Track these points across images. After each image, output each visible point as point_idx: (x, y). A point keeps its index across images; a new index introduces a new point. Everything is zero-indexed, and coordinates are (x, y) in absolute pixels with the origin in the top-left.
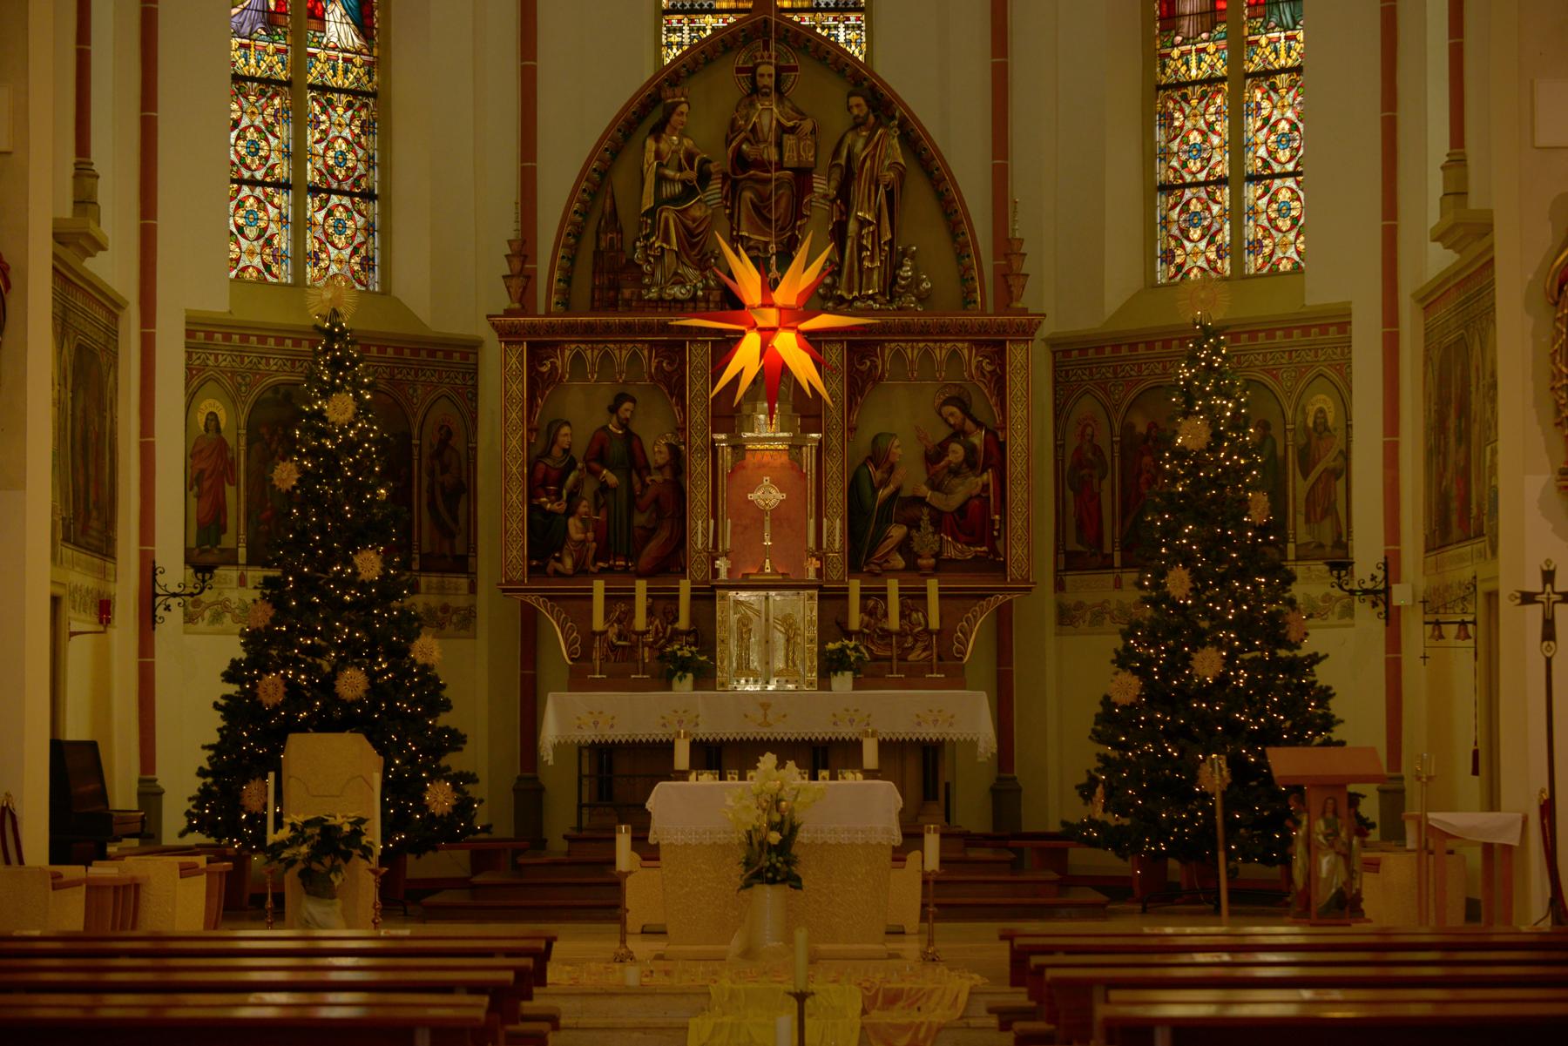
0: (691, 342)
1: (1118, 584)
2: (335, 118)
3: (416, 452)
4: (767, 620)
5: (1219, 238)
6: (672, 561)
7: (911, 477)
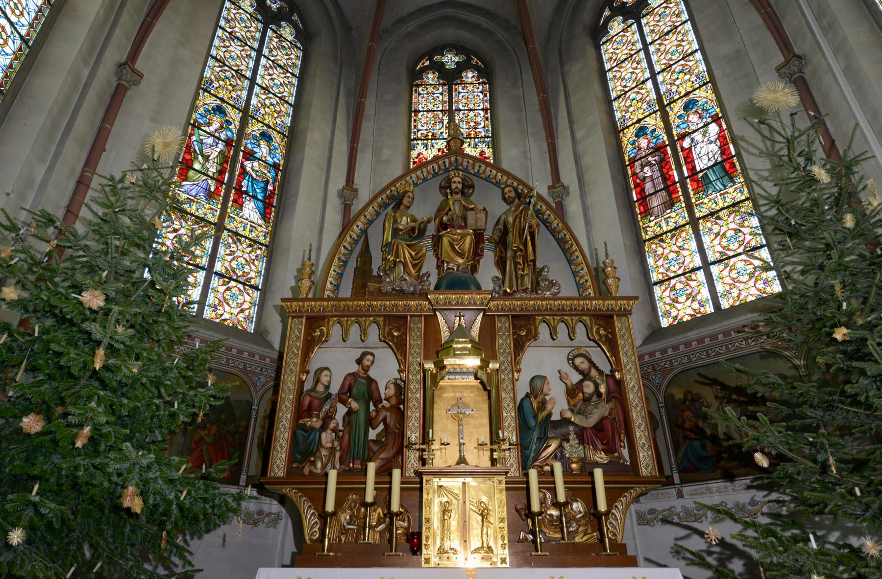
0: (411, 316)
1: (680, 495)
2: (240, 247)
3: (254, 413)
4: (465, 502)
5: (699, 297)
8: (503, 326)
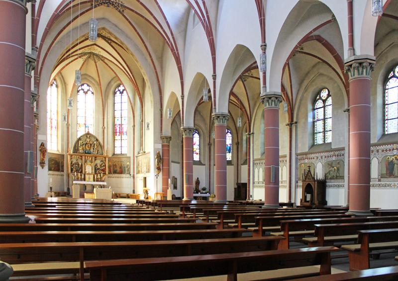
6: (81, 172)
7: (99, 167)
8: (94, 158)
